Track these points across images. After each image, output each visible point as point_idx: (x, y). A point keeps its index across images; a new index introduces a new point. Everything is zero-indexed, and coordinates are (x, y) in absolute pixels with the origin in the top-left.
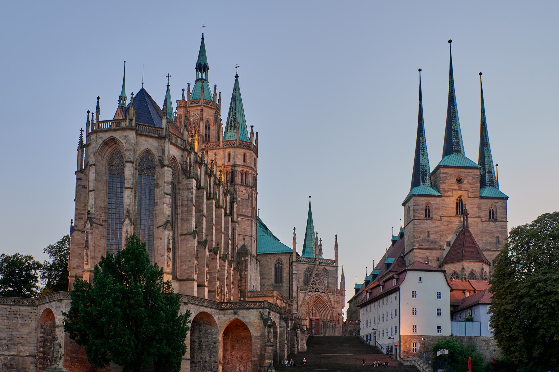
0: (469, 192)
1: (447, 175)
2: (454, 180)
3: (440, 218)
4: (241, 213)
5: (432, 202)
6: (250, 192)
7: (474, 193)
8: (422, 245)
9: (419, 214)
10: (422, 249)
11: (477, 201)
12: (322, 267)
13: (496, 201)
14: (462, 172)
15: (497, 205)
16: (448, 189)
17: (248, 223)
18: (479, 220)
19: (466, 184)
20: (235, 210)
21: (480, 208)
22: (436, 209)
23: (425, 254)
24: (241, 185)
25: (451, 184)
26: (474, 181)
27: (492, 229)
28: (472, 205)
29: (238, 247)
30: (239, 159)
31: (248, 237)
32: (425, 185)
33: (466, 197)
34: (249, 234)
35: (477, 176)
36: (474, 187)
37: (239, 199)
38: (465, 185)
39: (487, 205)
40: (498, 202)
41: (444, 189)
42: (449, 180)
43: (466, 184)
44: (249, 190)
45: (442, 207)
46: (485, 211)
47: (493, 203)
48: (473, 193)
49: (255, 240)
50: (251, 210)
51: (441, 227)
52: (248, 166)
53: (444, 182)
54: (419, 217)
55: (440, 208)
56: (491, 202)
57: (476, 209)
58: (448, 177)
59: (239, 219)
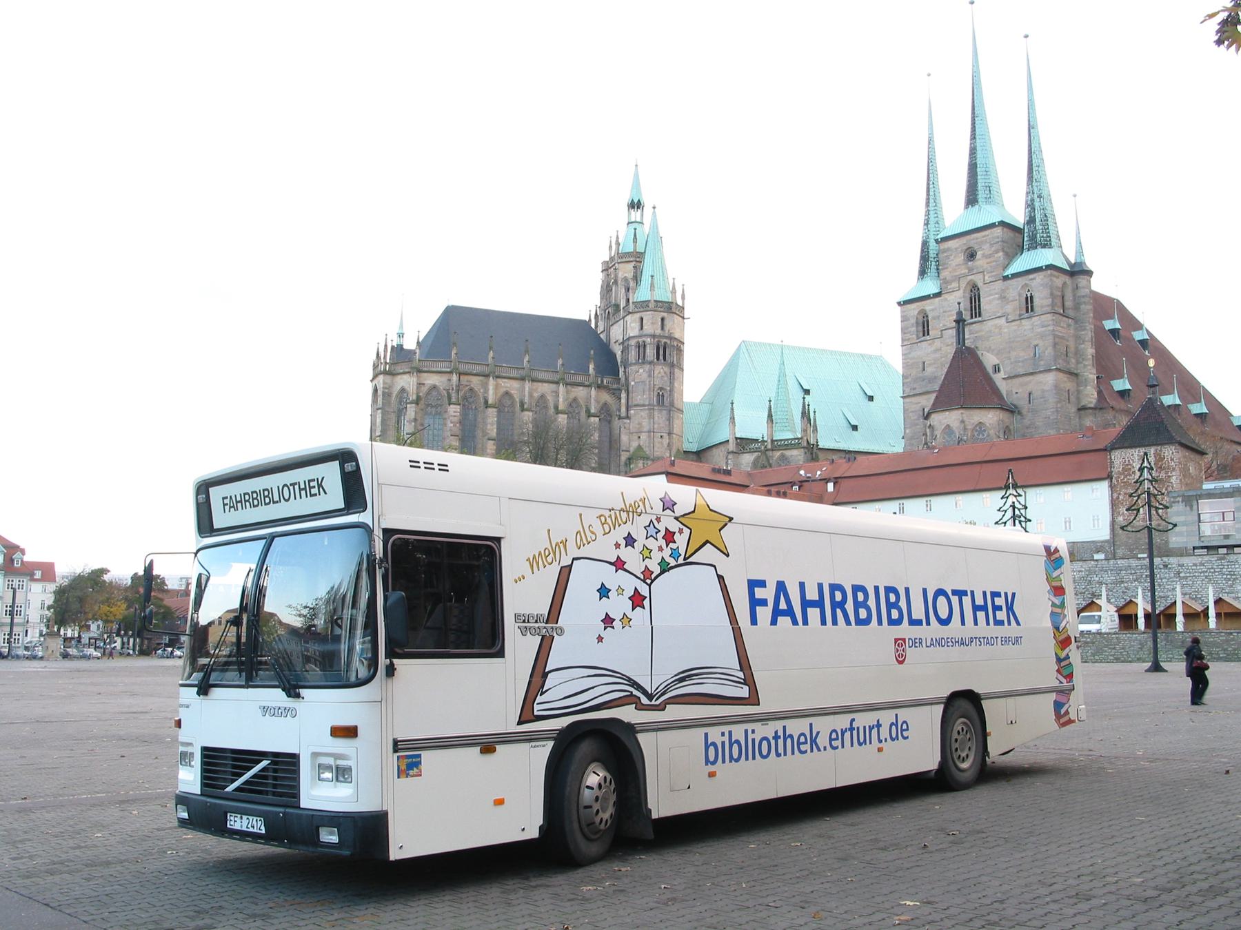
0: (985, 273)
1: (950, 253)
2: (961, 258)
3: (940, 333)
4: (636, 403)
5: (928, 308)
6: (647, 370)
7: (993, 272)
8: (914, 389)
9: (908, 335)
10: (914, 395)
11: (1000, 284)
12: (778, 454)
13: (1031, 276)
14: (973, 239)
15: (1034, 284)
16: (952, 277)
17: (644, 414)
18: (1002, 321)
19: (979, 259)
20: (623, 401)
21: (1005, 298)
22: (934, 318)
23: (919, 403)
24: (635, 364)
25: (957, 267)
26: (993, 249)
27: (1026, 333)
28: (991, 295)
29: (629, 451)
30: (632, 329)
31: (643, 434)
32: (924, 279)
33: (981, 284)
34: (645, 429)
35: (998, 240)
36: (993, 262)
37: (633, 383)
38: (980, 261)
39: (1015, 290)
40: (1034, 279)
41: (946, 279)
42: (952, 260)
43: (979, 259)
44: (647, 367)
45: (944, 312)
46: (1012, 301)
47: (1027, 282)
48: (992, 272)
49: (665, 435)
50: (650, 394)
51: (942, 349)
52: (645, 335)
53: (946, 266)
54: (909, 339)
55: (939, 316)
56: (1021, 281)
57: (998, 302)
58: (951, 255)
59: (632, 412)
